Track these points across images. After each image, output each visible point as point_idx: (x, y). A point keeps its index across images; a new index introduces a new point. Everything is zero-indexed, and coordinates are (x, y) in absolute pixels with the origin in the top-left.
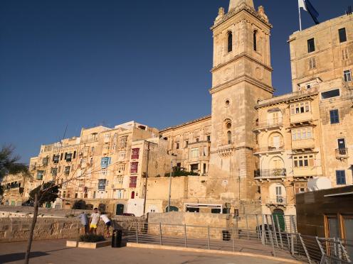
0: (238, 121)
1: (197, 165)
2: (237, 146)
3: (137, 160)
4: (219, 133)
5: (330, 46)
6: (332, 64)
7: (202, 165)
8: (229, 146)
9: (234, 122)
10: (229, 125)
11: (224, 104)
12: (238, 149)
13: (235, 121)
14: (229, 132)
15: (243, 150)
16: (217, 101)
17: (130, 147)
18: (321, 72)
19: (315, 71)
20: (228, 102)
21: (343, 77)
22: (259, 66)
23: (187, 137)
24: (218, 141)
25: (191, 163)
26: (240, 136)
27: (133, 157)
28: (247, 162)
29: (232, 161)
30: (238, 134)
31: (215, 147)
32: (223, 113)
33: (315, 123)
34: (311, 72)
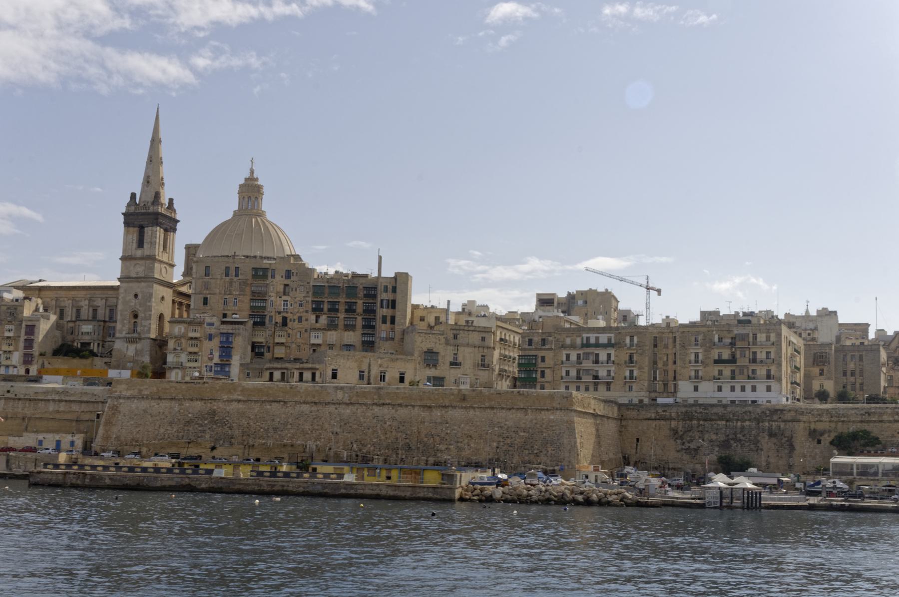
0: (145, 315)
1: (89, 344)
2: (143, 336)
3: (32, 337)
4: (125, 322)
5: (219, 277)
6: (218, 291)
7: (96, 345)
8: (135, 335)
9: (141, 315)
10: (136, 316)
11: (132, 297)
12: (144, 339)
13: (143, 315)
14: (135, 322)
15: (149, 341)
16: (125, 291)
17: (21, 321)
18: (211, 294)
19: (208, 292)
20: (136, 296)
21: (223, 302)
22: (165, 265)
23: (62, 304)
24: (124, 328)
25: (82, 341)
26: (146, 328)
27: (26, 333)
28: (151, 351)
29: (138, 348)
30: (145, 326)
31: (121, 333)
32: (133, 304)
33: (201, 339)
34: (205, 292)
